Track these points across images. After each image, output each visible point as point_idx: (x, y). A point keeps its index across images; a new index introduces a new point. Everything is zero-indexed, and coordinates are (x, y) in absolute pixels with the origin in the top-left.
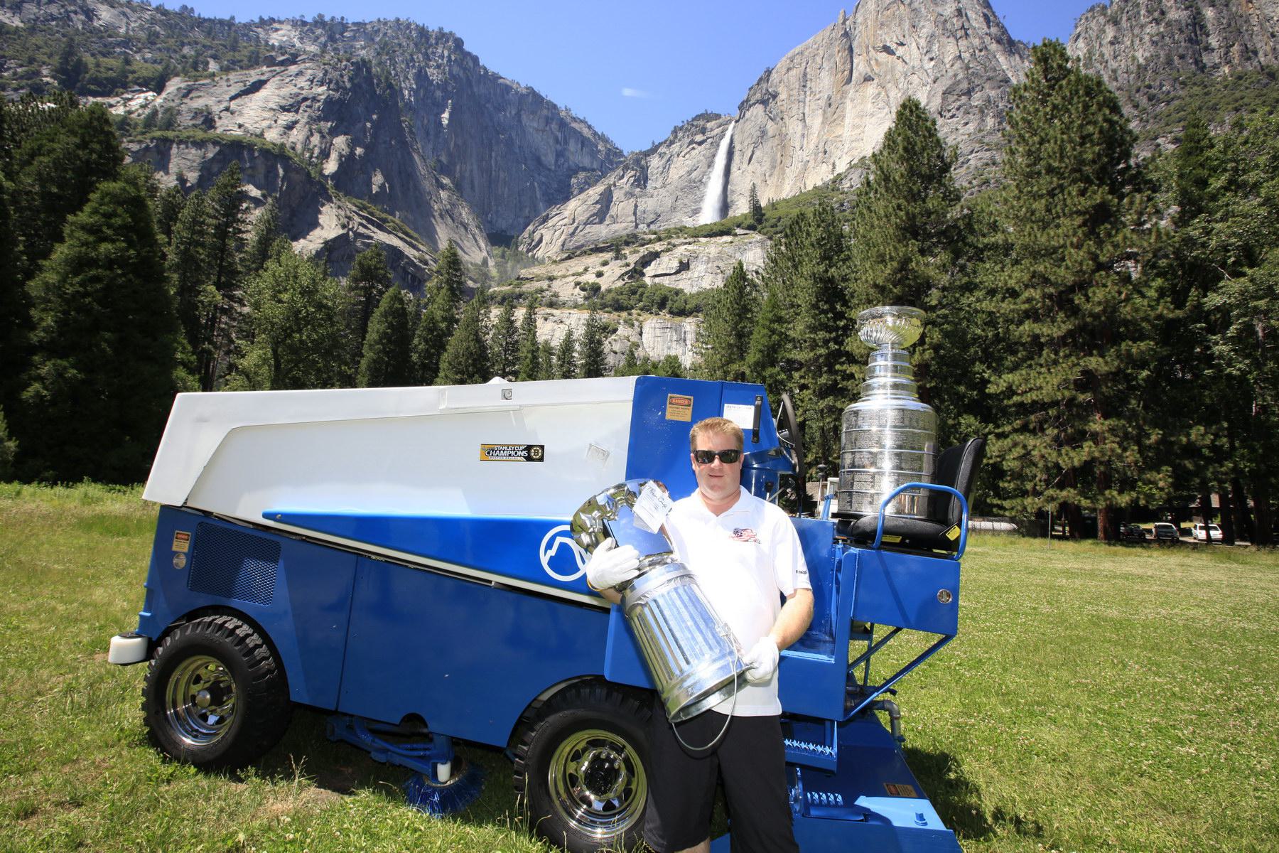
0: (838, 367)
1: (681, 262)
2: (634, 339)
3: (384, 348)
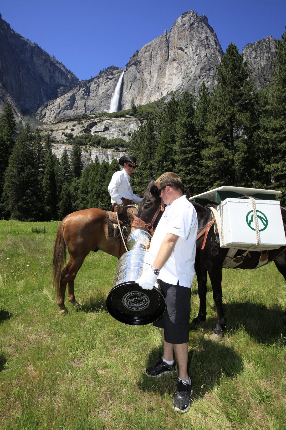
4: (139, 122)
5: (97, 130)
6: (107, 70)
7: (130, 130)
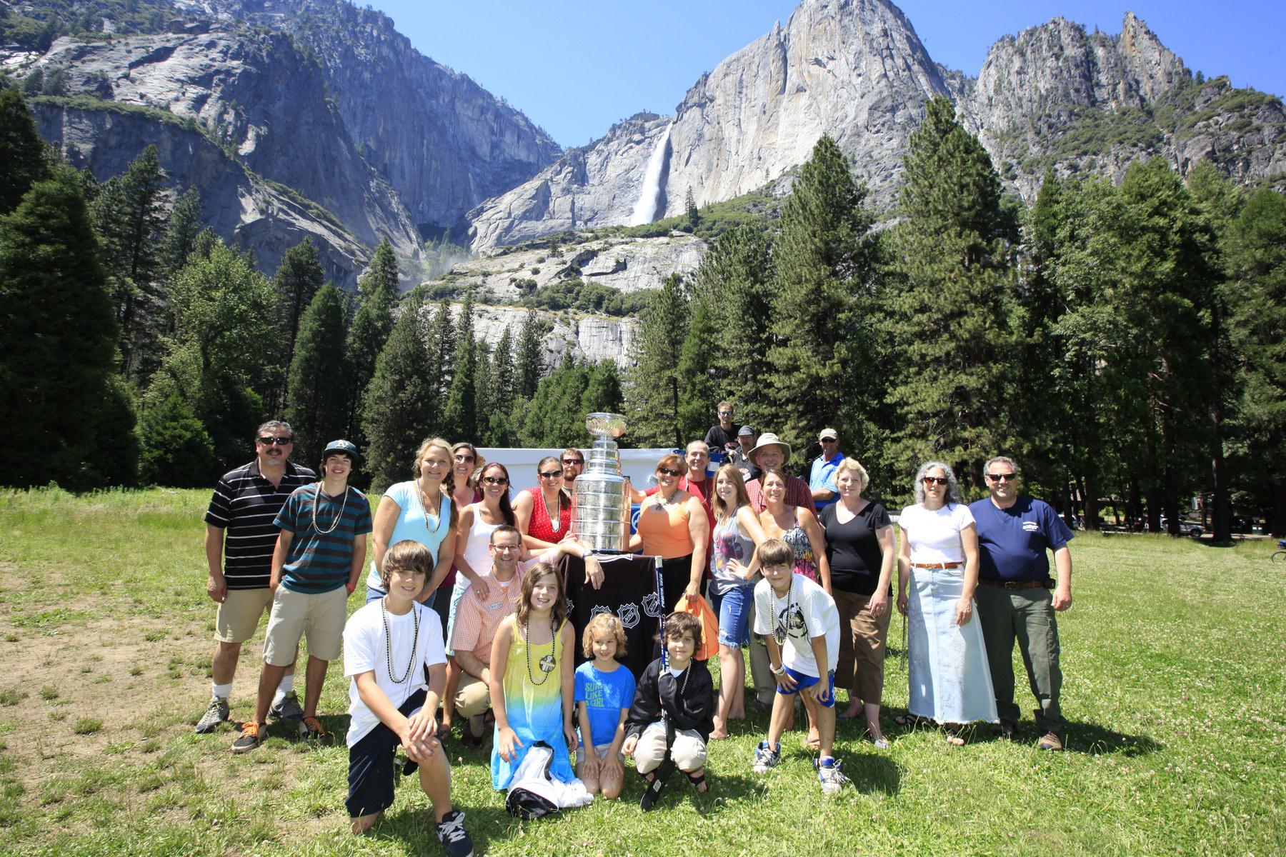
0: (759, 377)
1: (618, 262)
2: (570, 338)
3: (318, 347)
4: (705, 246)
5: (595, 272)
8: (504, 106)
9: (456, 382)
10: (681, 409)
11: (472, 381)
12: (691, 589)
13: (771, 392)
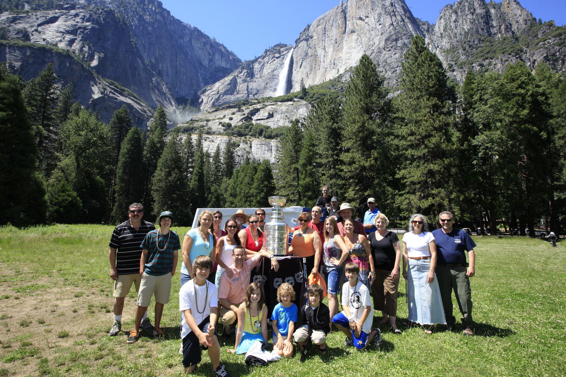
0: (337, 167)
1: (269, 114)
4: (310, 106)
5: (259, 118)
6: (273, 48)
7: (298, 116)
8: (215, 42)
9: (195, 172)
10: (300, 183)
11: (203, 171)
12: (314, 270)
13: (342, 174)
